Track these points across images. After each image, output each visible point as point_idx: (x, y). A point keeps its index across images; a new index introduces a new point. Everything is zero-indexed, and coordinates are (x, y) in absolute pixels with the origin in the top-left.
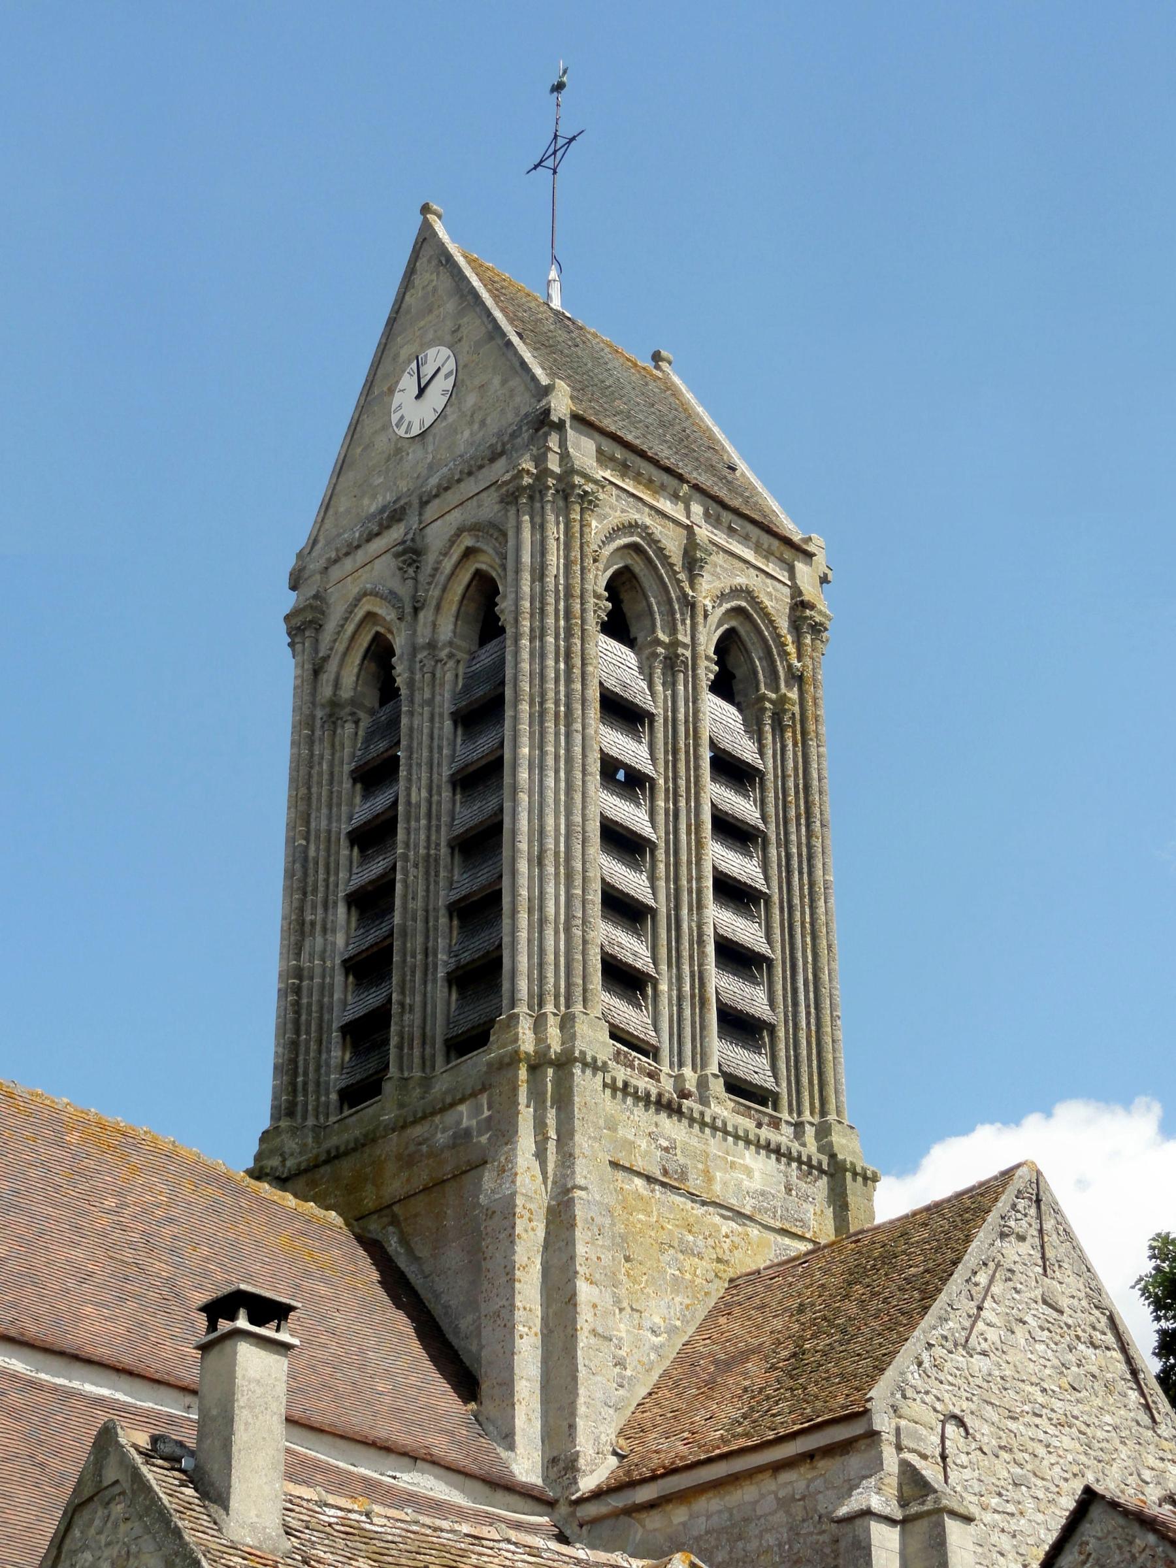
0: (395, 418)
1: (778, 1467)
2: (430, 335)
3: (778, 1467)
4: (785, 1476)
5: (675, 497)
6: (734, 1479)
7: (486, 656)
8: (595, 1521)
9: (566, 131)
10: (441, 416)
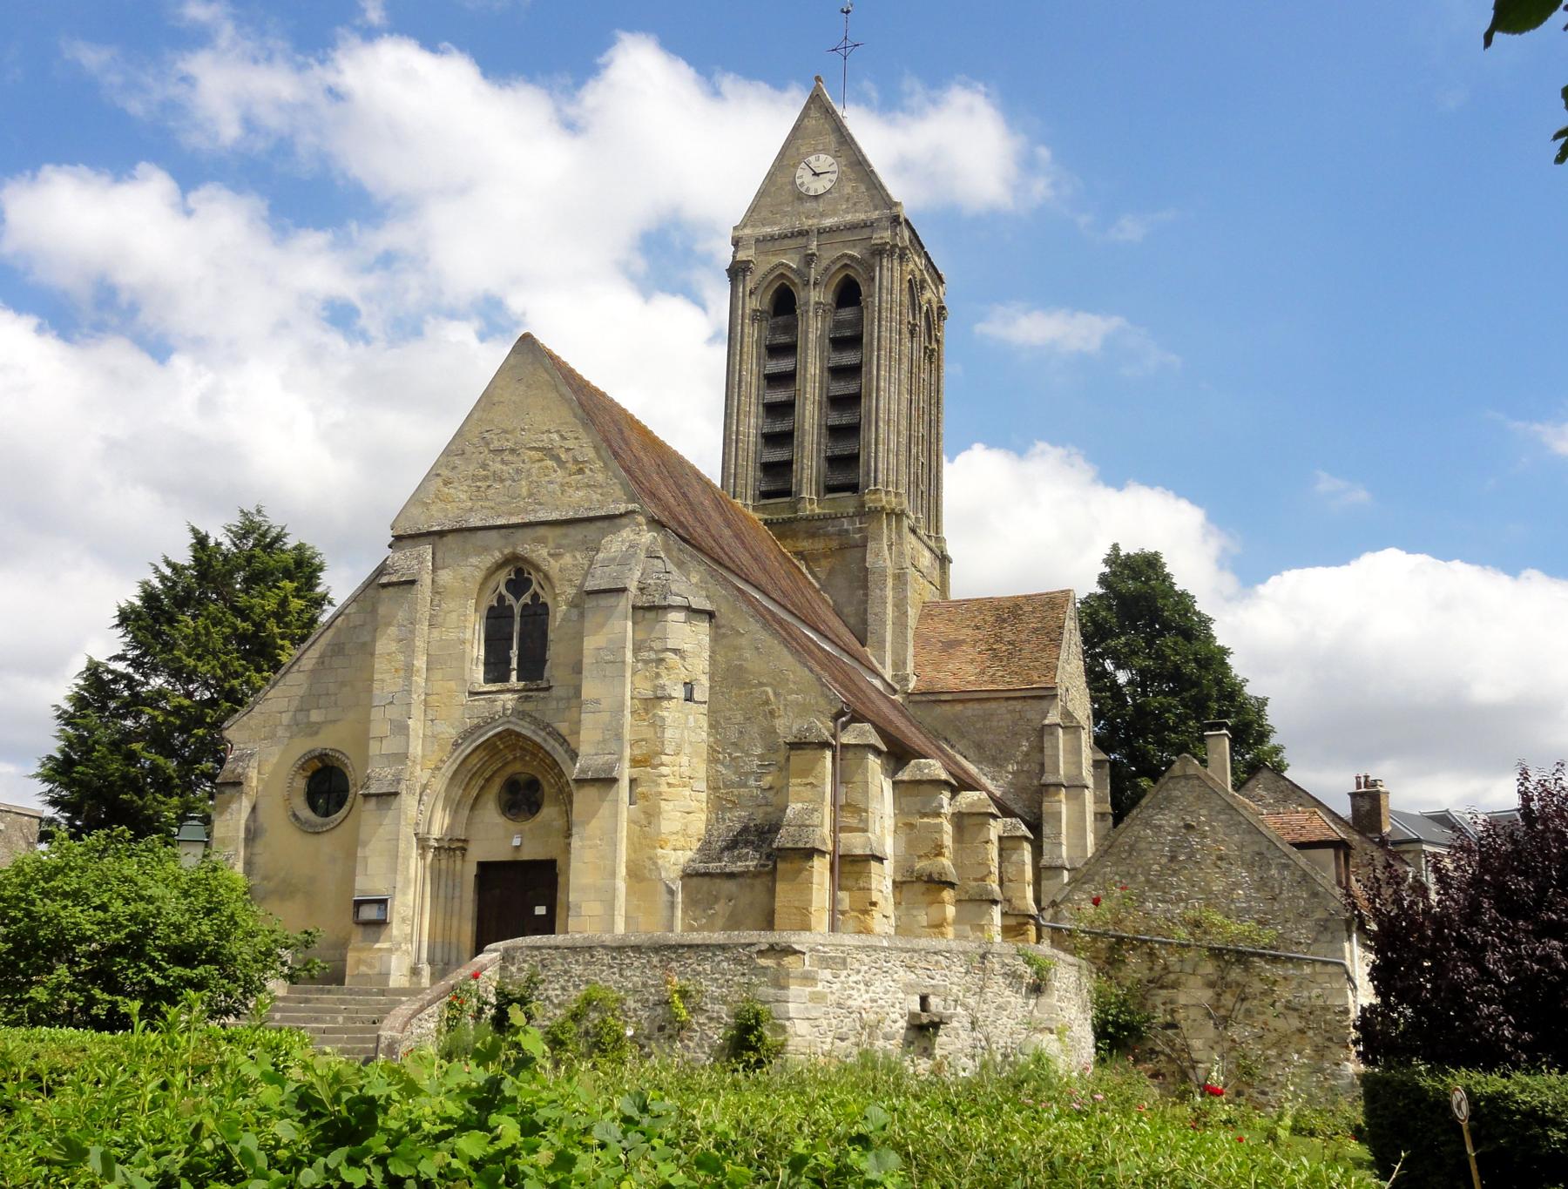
1: (1008, 699)
2: (821, 147)
3: (1008, 699)
4: (1011, 702)
5: (919, 256)
6: (988, 699)
7: (847, 314)
8: (916, 702)
9: (853, 39)
10: (829, 191)
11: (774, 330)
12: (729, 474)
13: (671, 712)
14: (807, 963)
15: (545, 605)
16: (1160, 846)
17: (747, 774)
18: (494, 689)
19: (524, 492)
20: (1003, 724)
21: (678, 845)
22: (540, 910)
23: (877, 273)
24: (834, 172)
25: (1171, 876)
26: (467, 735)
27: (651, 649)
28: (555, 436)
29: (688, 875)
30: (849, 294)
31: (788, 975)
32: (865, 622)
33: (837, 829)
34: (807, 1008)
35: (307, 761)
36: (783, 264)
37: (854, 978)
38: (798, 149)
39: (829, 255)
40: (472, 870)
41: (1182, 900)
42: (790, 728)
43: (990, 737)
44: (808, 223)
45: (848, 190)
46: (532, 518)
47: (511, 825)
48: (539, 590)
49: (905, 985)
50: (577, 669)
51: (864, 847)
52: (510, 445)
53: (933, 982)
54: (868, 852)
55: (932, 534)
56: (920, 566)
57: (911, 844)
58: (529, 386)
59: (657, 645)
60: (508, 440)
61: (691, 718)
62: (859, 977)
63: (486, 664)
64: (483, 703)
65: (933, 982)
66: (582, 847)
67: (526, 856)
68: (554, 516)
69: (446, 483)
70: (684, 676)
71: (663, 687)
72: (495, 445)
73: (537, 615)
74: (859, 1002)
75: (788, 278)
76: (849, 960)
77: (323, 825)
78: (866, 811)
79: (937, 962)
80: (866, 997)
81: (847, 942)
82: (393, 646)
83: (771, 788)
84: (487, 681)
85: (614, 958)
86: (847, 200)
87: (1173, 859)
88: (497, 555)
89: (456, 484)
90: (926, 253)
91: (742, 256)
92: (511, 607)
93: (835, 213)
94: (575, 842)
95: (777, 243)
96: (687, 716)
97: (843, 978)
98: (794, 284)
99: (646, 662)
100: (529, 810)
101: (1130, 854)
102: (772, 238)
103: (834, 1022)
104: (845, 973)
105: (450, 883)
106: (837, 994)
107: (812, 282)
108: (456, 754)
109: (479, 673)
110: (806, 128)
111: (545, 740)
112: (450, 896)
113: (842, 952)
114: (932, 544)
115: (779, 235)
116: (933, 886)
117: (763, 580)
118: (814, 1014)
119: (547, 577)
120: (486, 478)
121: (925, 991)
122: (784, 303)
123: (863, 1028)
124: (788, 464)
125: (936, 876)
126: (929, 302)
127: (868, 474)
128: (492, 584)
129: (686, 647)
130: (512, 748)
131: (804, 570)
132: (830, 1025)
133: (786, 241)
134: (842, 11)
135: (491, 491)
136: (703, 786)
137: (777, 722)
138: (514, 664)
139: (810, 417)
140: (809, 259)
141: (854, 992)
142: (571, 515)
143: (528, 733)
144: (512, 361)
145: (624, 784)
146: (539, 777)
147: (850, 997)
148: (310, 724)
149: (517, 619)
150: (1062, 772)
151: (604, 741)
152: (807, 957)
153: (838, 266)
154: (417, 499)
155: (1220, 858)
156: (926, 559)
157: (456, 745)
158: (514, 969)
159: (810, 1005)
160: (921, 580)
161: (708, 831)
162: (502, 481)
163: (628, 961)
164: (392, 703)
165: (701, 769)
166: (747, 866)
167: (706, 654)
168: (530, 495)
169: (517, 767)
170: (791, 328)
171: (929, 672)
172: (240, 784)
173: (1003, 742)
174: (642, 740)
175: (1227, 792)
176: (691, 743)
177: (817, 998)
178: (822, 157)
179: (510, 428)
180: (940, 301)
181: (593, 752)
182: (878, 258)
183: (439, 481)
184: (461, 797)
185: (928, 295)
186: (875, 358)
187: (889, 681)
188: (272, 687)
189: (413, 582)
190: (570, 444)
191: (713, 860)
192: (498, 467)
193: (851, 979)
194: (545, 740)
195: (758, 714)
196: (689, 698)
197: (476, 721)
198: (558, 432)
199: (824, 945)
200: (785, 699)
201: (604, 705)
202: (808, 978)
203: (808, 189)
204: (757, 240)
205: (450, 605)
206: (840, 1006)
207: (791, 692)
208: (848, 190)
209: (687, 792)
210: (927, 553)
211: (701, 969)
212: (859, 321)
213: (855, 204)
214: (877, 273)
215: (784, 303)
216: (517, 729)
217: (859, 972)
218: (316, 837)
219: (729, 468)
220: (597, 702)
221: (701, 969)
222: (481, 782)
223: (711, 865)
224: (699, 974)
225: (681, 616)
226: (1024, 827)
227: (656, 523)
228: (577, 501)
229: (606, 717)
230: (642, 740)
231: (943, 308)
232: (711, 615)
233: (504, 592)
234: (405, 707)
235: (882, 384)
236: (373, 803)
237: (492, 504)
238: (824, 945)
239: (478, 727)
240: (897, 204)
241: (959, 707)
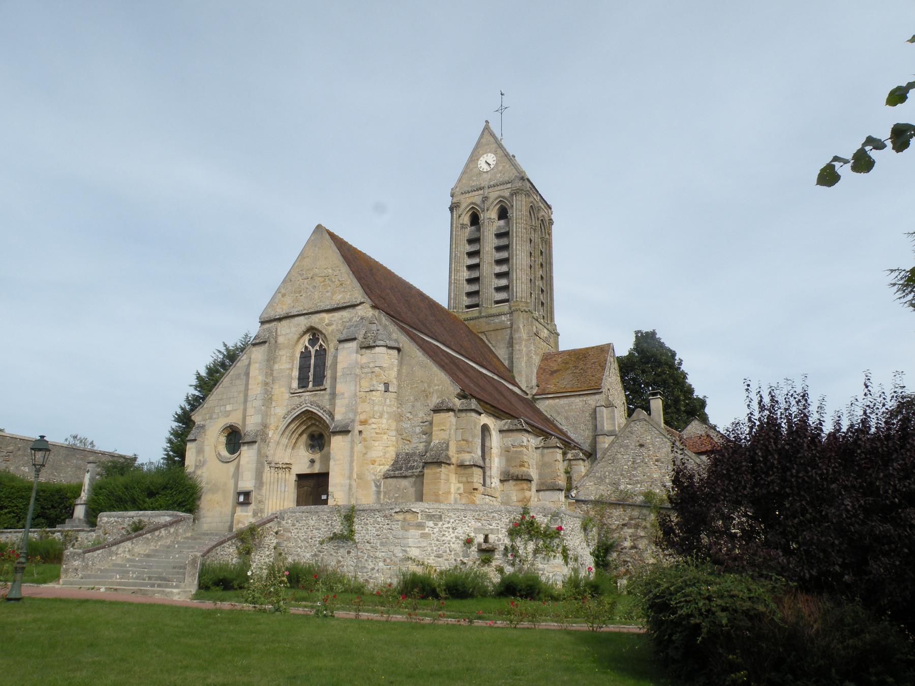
0: (479, 166)
12: (451, 298)
13: (377, 396)
14: (419, 518)
15: (325, 349)
16: (628, 456)
18: (301, 391)
19: (316, 297)
20: (578, 407)
21: (381, 463)
23: (515, 203)
25: (633, 471)
27: (369, 367)
28: (330, 271)
29: (386, 477)
30: (503, 214)
31: (409, 524)
32: (512, 362)
33: (459, 452)
34: (419, 542)
35: (223, 430)
37: (446, 525)
38: (479, 152)
39: (493, 195)
40: (294, 478)
41: (638, 483)
43: (572, 413)
48: (322, 343)
49: (475, 529)
50: (334, 379)
51: (470, 461)
52: (310, 276)
53: (491, 527)
54: (472, 463)
55: (549, 322)
56: (542, 337)
57: (509, 460)
58: (319, 248)
59: (372, 365)
60: (310, 274)
61: (388, 401)
62: (449, 525)
63: (299, 379)
65: (491, 527)
66: (335, 465)
70: (384, 378)
71: (373, 386)
72: (305, 276)
73: (322, 354)
74: (449, 538)
76: (443, 516)
77: (230, 459)
78: (471, 442)
79: (493, 517)
80: (453, 535)
81: (442, 507)
82: (257, 372)
84: (299, 388)
85: (328, 517)
86: (501, 173)
87: (634, 462)
88: (304, 328)
90: (540, 195)
91: (455, 200)
92: (310, 351)
96: (386, 399)
97: (440, 526)
99: (366, 373)
100: (320, 449)
101: (613, 462)
103: (435, 548)
104: (441, 523)
105: (283, 484)
106: (437, 534)
107: (486, 210)
109: (295, 384)
112: (283, 491)
113: (439, 512)
114: (549, 327)
116: (519, 482)
117: (426, 331)
118: (424, 544)
121: (486, 533)
122: (475, 220)
123: (451, 551)
125: (520, 476)
126: (543, 216)
127: (513, 294)
128: (302, 341)
129: (385, 365)
130: (310, 418)
131: (485, 339)
132: (432, 550)
133: (474, 193)
135: (302, 297)
136: (394, 433)
138: (311, 378)
139: (489, 269)
140: (485, 199)
141: (446, 533)
144: (312, 238)
145: (356, 432)
146: (323, 433)
147: (444, 535)
148: (226, 411)
149: (313, 358)
150: (605, 429)
152: (419, 515)
154: (271, 304)
155: (657, 461)
156: (545, 333)
158: (284, 522)
159: (421, 539)
160: (543, 343)
161: (397, 456)
162: (306, 292)
163: (334, 518)
165: (394, 425)
166: (412, 472)
167: (395, 369)
169: (314, 428)
170: (479, 230)
171: (543, 385)
173: (578, 416)
174: (364, 412)
175: (660, 426)
176: (388, 413)
177: (424, 536)
178: (489, 154)
180: (549, 216)
182: (514, 196)
183: (280, 295)
184: (288, 443)
185: (542, 213)
186: (514, 241)
187: (524, 389)
189: (265, 342)
191: (398, 470)
193: (444, 526)
196: (387, 390)
199: (429, 509)
200: (433, 389)
201: (346, 395)
202: (420, 526)
203: (483, 169)
205: (282, 352)
206: (438, 540)
207: (435, 385)
208: (500, 168)
209: (385, 437)
210: (546, 331)
211: (368, 522)
213: (504, 174)
214: (515, 203)
215: (475, 220)
216: (311, 409)
217: (449, 522)
220: (343, 394)
221: (368, 522)
222: (297, 436)
223: (396, 473)
224: (367, 524)
225: (383, 350)
226: (581, 454)
227: (375, 307)
228: (339, 298)
229: (346, 401)
230: (364, 412)
231: (551, 219)
232: (399, 350)
233: (307, 345)
235: (518, 252)
238: (429, 509)
241: (557, 401)
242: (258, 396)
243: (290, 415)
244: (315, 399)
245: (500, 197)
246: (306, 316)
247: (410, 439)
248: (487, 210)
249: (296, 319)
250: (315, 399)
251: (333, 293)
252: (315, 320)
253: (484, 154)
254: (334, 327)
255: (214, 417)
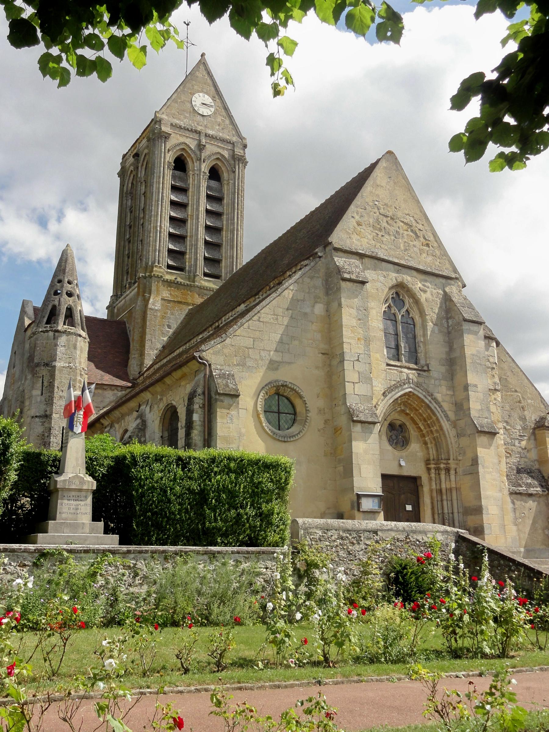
11: (174, 177)
17: (514, 439)
22: (409, 508)
24: (212, 106)
26: (390, 389)
27: (489, 361)
28: (412, 219)
36: (186, 144)
38: (193, 86)
39: (211, 149)
42: (531, 418)
44: (199, 128)
45: (219, 119)
46: (410, 264)
47: (396, 452)
52: (390, 214)
58: (395, 183)
64: (396, 372)
67: (405, 473)
68: (421, 267)
69: (359, 224)
72: (382, 211)
75: (187, 152)
82: (354, 322)
83: (525, 449)
86: (219, 125)
88: (394, 282)
89: (364, 227)
93: (213, 129)
94: (481, 470)
95: (182, 130)
98: (189, 155)
102: (180, 127)
108: (384, 402)
110: (197, 77)
111: (430, 402)
115: (184, 127)
119: (417, 302)
120: (380, 230)
124: (182, 254)
133: (187, 132)
134: (185, 23)
137: (526, 413)
142: (429, 270)
143: (422, 397)
146: (407, 424)
151: (482, 409)
153: (215, 157)
157: (384, 394)
162: (389, 235)
164: (358, 360)
168: (406, 250)
170: (185, 180)
172: (237, 396)
179: (389, 204)
181: (477, 416)
188: (240, 327)
190: (420, 227)
192: (384, 224)
194: (430, 402)
195: (517, 407)
197: (393, 383)
198: (413, 217)
201: (480, 388)
204: (172, 125)
207: (529, 398)
212: (221, 190)
213: (223, 129)
216: (416, 393)
218: (283, 444)
219: (156, 246)
220: (476, 386)
234: (367, 365)
236: (359, 427)
237: (386, 248)
239: (395, 387)
240: (244, 138)
242: (361, 356)
243: (390, 395)
244: (421, 380)
245: (219, 153)
246: (396, 267)
247: (510, 452)
248: (204, 162)
249: (384, 264)
250: (421, 380)
251: (421, 251)
252: (407, 278)
253: (199, 92)
254: (428, 295)
255: (249, 363)
